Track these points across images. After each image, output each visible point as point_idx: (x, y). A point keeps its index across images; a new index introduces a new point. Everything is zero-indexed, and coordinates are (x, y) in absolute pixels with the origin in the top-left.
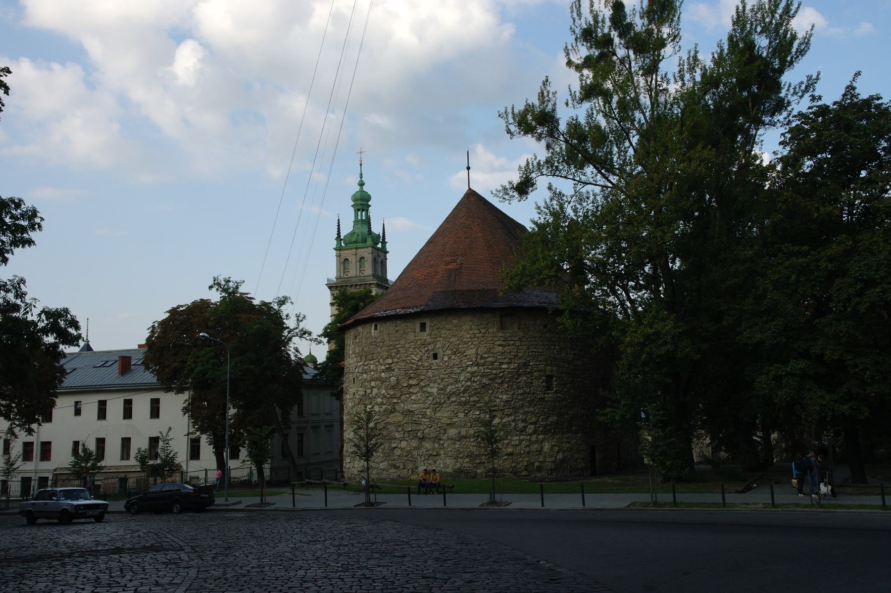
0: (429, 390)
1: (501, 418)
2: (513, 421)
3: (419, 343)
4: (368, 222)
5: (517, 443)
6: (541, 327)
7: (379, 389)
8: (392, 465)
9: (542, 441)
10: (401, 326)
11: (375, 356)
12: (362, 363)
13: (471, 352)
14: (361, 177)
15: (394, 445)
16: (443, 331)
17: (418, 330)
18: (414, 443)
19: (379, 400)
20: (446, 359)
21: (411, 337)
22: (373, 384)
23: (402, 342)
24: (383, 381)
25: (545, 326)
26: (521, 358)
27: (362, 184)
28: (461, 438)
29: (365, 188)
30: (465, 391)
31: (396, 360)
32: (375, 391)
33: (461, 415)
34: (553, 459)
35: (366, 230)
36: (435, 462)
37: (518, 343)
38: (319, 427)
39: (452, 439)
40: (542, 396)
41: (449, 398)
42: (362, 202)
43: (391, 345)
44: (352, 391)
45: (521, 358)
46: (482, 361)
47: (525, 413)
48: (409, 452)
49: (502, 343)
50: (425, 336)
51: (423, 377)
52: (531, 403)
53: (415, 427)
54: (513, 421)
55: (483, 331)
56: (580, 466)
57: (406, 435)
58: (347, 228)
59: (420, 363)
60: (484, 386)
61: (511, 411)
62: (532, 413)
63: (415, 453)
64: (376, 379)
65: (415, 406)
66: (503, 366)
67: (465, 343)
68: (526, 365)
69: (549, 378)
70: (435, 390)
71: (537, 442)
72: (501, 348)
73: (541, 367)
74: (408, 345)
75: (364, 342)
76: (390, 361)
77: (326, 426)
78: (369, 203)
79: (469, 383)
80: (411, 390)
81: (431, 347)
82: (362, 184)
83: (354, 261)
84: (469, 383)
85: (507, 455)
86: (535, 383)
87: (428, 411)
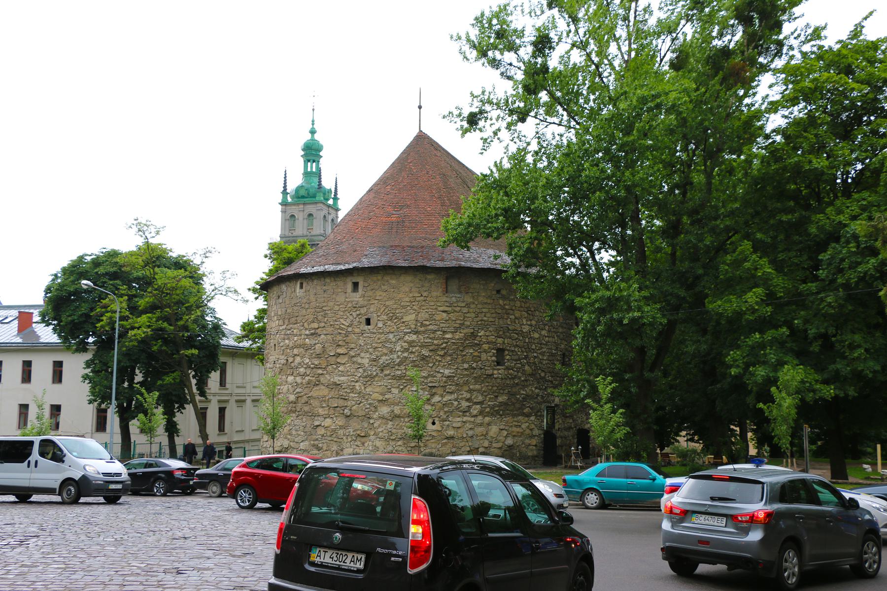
0: (360, 360)
1: (442, 396)
2: (456, 400)
3: (350, 305)
4: (318, 174)
5: (459, 425)
6: (494, 292)
7: (302, 358)
8: (314, 445)
9: (489, 424)
10: (330, 284)
11: (299, 319)
12: (284, 327)
13: (410, 318)
14: (313, 124)
15: (317, 423)
16: (379, 293)
17: (350, 287)
18: (341, 421)
19: (302, 370)
20: (380, 325)
21: (341, 298)
22: (296, 351)
23: (331, 304)
24: (307, 348)
25: (498, 292)
26: (468, 327)
27: (313, 132)
28: (395, 417)
29: (316, 136)
30: (399, 365)
31: (322, 325)
32: (298, 359)
33: (395, 391)
34: (500, 445)
35: (315, 184)
36: (363, 444)
37: (465, 310)
38: (244, 401)
39: (383, 418)
40: (490, 372)
41: (382, 370)
42: (312, 152)
44: (272, 359)
45: (468, 327)
46: (422, 329)
47: (470, 391)
48: (334, 431)
49: (447, 309)
50: (356, 297)
51: (353, 346)
52: (477, 380)
53: (341, 403)
54: (456, 400)
55: (425, 294)
56: (530, 454)
57: (332, 411)
58: (296, 181)
59: (350, 329)
60: (424, 358)
61: (453, 388)
62: (478, 391)
63: (341, 432)
65: (342, 378)
66: (447, 336)
67: (404, 307)
68: (473, 335)
69: (500, 351)
70: (366, 361)
71: (481, 425)
72: (445, 315)
73: (492, 339)
74: (337, 308)
75: (287, 302)
76: (315, 325)
77: (253, 401)
78: (321, 154)
79: (406, 354)
80: (339, 360)
81: (363, 311)
82: (313, 132)
83: (301, 219)
84: (406, 354)
85: (447, 438)
86: (484, 356)
87: (357, 384)
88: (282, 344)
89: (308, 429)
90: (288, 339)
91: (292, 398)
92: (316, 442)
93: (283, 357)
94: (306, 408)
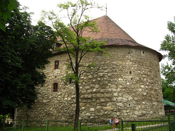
7: (147, 79)
15: (154, 104)
22: (144, 76)
24: (148, 76)
32: (145, 80)
87: (160, 91)
88: (136, 72)
89: (151, 106)
90: (140, 71)
91: (145, 94)
92: (155, 111)
93: (137, 77)
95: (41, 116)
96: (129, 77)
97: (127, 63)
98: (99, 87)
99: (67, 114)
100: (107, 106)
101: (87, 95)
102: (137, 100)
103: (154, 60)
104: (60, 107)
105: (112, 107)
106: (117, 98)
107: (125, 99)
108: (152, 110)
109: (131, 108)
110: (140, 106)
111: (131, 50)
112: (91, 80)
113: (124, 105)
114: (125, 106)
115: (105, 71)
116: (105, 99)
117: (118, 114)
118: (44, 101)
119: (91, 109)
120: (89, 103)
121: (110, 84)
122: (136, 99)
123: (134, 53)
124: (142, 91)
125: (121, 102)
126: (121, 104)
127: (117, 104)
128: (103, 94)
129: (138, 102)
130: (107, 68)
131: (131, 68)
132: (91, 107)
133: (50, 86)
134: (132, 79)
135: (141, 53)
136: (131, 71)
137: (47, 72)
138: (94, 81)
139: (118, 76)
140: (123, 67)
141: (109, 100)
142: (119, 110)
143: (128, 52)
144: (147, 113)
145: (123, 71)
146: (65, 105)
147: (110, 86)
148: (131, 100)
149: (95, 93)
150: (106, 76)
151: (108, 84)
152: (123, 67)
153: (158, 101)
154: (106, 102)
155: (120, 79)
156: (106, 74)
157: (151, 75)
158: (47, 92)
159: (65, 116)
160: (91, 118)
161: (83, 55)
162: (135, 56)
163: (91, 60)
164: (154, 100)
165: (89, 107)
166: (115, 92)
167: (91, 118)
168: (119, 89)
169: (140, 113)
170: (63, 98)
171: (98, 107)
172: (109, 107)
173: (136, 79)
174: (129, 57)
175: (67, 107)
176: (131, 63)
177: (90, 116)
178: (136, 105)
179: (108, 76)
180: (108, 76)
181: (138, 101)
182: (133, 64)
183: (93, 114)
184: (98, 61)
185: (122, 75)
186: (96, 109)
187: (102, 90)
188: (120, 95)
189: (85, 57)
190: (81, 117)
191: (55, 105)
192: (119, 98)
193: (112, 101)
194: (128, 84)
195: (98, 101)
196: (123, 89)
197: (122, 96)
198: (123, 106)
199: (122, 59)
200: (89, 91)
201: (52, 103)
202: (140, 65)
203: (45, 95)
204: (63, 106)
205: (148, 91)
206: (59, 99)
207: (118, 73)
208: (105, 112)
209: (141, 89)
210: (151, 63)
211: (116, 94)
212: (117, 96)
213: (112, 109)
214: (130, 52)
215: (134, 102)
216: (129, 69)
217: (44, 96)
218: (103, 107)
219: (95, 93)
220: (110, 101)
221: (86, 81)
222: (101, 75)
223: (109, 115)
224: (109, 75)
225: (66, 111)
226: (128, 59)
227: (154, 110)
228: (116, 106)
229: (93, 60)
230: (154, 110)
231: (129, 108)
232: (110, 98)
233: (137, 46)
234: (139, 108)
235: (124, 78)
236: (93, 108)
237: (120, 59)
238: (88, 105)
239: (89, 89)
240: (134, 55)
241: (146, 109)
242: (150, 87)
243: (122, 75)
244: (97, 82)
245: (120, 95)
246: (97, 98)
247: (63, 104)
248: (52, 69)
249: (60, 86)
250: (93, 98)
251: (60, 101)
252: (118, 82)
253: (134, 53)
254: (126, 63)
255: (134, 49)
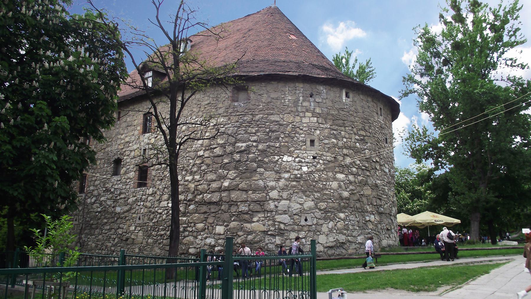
15: (368, 218)
19: (354, 169)
22: (345, 151)
24: (357, 151)
31: (369, 134)
32: (348, 160)
43: (366, 119)
63: (379, 226)
64: (350, 148)
65: (379, 182)
70: (387, 171)
87: (386, 188)
88: (326, 141)
90: (336, 138)
91: (346, 194)
94: (358, 205)
95: (110, 244)
96: (308, 152)
97: (305, 120)
98: (237, 177)
99: (164, 241)
100: (254, 222)
101: (210, 196)
102: (325, 208)
103: (375, 114)
104: (151, 224)
105: (264, 225)
106: (276, 203)
107: (295, 207)
108: (361, 233)
109: (310, 227)
110: (332, 222)
111: (317, 87)
112: (219, 160)
113: (293, 219)
114: (295, 223)
115: (253, 139)
116: (249, 205)
117: (278, 240)
118: (118, 209)
119: (217, 229)
120: (213, 215)
121: (262, 170)
122: (323, 205)
123: (324, 95)
124: (340, 186)
125: (285, 212)
126: (285, 218)
127: (276, 217)
128: (244, 192)
129: (328, 214)
130: (257, 131)
131: (313, 130)
132: (217, 225)
133: (131, 174)
134: (314, 158)
135: (340, 97)
136: (313, 138)
137: (127, 139)
138: (226, 161)
139: (284, 149)
140: (294, 128)
141: (259, 207)
142: (281, 233)
143: (308, 93)
144: (350, 242)
145: (296, 138)
146: (161, 219)
147: (261, 174)
148: (310, 209)
149: (228, 189)
150: (254, 150)
151: (258, 170)
152: (294, 128)
153: (380, 214)
154: (252, 213)
155: (285, 158)
156: (254, 144)
157: (365, 149)
158: (124, 187)
159: (160, 244)
160: (216, 249)
161: (187, 97)
162: (326, 103)
163: (221, 111)
164: (369, 210)
165: (213, 223)
166: (273, 188)
167: (216, 249)
168: (282, 183)
169: (331, 239)
170: (157, 200)
171: (233, 224)
172: (257, 225)
173: (325, 158)
174: (310, 105)
175: (166, 222)
176: (316, 119)
177: (215, 246)
178: (321, 222)
179: (258, 150)
180: (258, 150)
181: (329, 212)
182: (320, 121)
183: (220, 241)
184: (238, 114)
185: (292, 149)
186: (228, 228)
187: (243, 185)
188: (285, 195)
189: (209, 104)
190: (195, 248)
191: (139, 219)
192: (283, 202)
193: (265, 211)
194: (305, 169)
195: (233, 209)
196: (293, 182)
197: (289, 199)
198: (291, 223)
199: (293, 109)
200: (214, 185)
201: (135, 213)
202: (337, 125)
203: (120, 195)
204: (157, 221)
205: (353, 188)
206: (149, 204)
207: (283, 144)
208: (248, 235)
209: (337, 182)
210: (366, 120)
211: (274, 194)
212: (277, 197)
213: (264, 228)
214: (314, 93)
215: (318, 214)
216: (309, 134)
217: (118, 198)
218: (245, 225)
219: (227, 190)
220: (260, 210)
221: (208, 161)
222: (243, 148)
223: (257, 242)
224: (260, 147)
225: (162, 233)
226: (307, 111)
227: (369, 233)
228: (274, 221)
229: (227, 112)
230: (369, 233)
231: (306, 229)
232: (261, 203)
233: (332, 79)
234: (330, 227)
235: (295, 156)
236: (221, 225)
237: (290, 109)
238: (210, 220)
239: (215, 181)
240: (324, 101)
241: (347, 230)
242: (360, 178)
243: (292, 149)
244: (233, 164)
245: (285, 195)
246: (233, 203)
247: (158, 216)
248: (136, 133)
249: (154, 173)
250: (223, 203)
251: (151, 209)
252: (281, 164)
253: (324, 95)
254: (303, 119)
255: (324, 85)
